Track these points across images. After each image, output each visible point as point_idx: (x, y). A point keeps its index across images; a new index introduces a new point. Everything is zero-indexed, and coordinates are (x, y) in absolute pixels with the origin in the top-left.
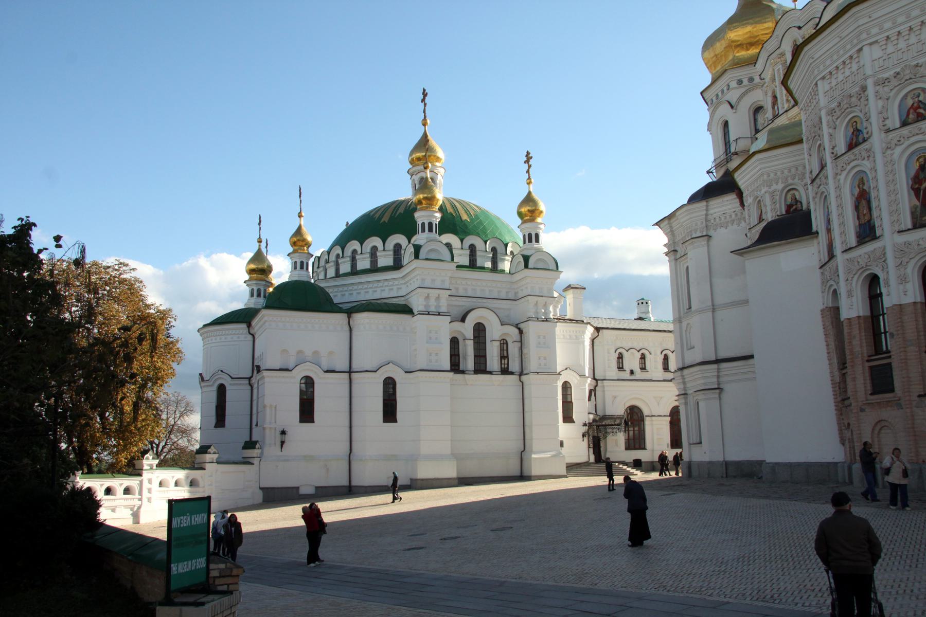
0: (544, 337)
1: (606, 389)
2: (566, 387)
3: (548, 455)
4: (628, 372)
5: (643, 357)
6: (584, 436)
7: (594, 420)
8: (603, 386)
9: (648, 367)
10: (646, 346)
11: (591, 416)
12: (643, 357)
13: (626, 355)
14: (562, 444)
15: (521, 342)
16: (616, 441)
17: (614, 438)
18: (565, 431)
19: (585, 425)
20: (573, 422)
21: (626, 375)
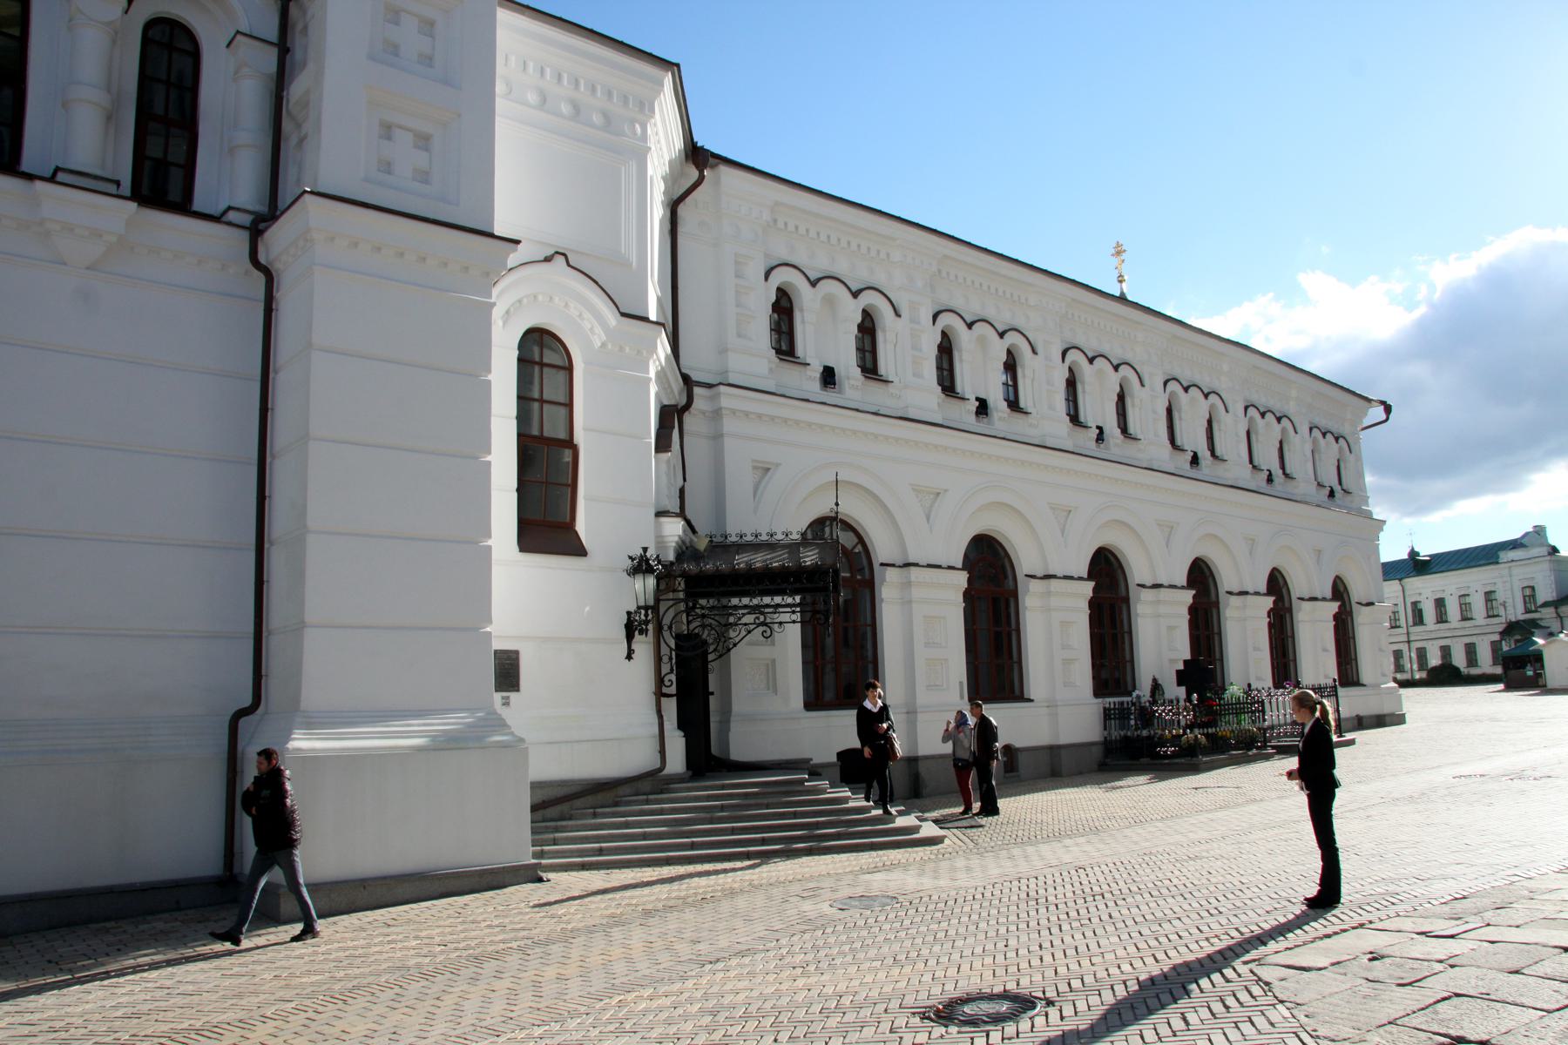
0: (428, 26)
1: (729, 425)
2: (541, 352)
3: (407, 736)
4: (816, 371)
5: (868, 329)
6: (631, 629)
7: (686, 552)
8: (717, 414)
9: (884, 367)
10: (879, 279)
11: (674, 529)
12: (868, 329)
13: (808, 303)
14: (507, 672)
15: (283, 47)
16: (771, 668)
17: (764, 652)
18: (524, 597)
19: (641, 566)
20: (579, 550)
21: (813, 386)
